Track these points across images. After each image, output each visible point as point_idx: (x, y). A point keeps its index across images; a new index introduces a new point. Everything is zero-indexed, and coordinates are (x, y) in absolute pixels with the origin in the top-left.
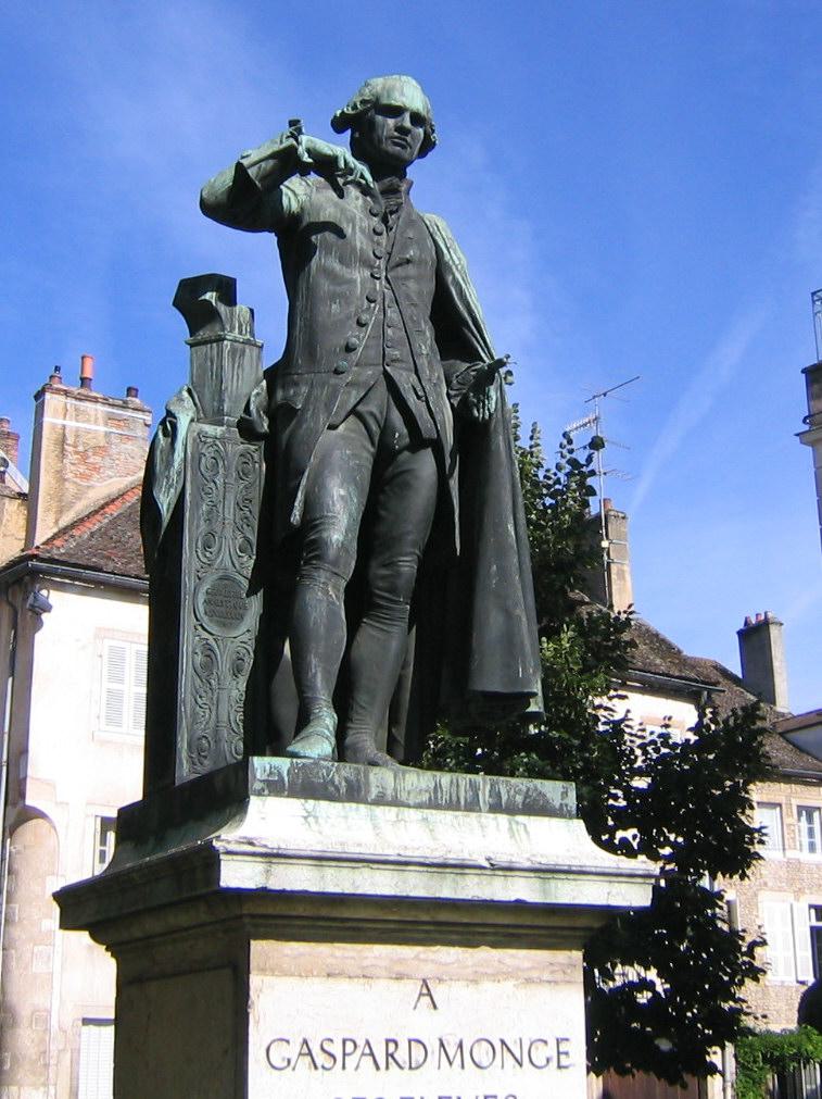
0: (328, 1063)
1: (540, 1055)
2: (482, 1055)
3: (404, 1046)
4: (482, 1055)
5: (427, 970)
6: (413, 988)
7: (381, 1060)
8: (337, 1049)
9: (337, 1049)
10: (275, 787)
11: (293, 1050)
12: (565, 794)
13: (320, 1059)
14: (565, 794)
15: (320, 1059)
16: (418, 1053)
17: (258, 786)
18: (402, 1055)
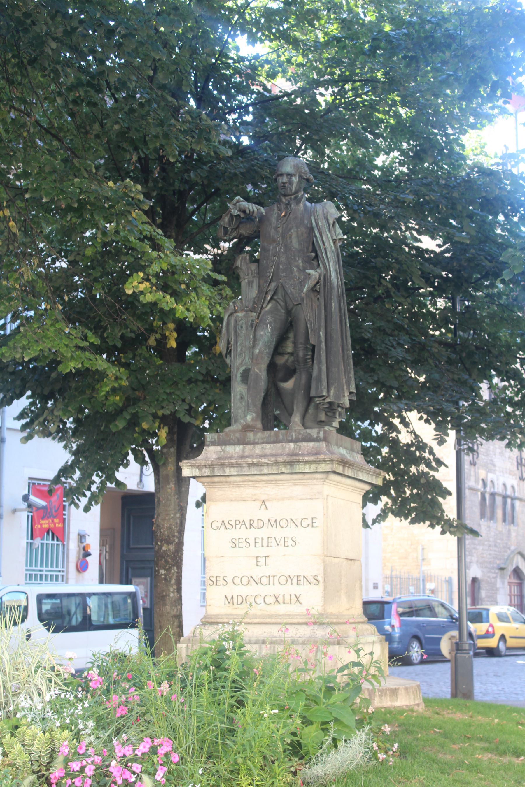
0: (230, 527)
1: (305, 524)
2: (284, 523)
3: (256, 522)
4: (284, 523)
5: (264, 497)
6: (259, 503)
7: (248, 526)
8: (233, 523)
9: (233, 523)
10: (213, 443)
11: (219, 524)
12: (318, 433)
13: (228, 526)
14: (318, 433)
15: (228, 526)
16: (261, 524)
17: (208, 443)
18: (255, 525)
